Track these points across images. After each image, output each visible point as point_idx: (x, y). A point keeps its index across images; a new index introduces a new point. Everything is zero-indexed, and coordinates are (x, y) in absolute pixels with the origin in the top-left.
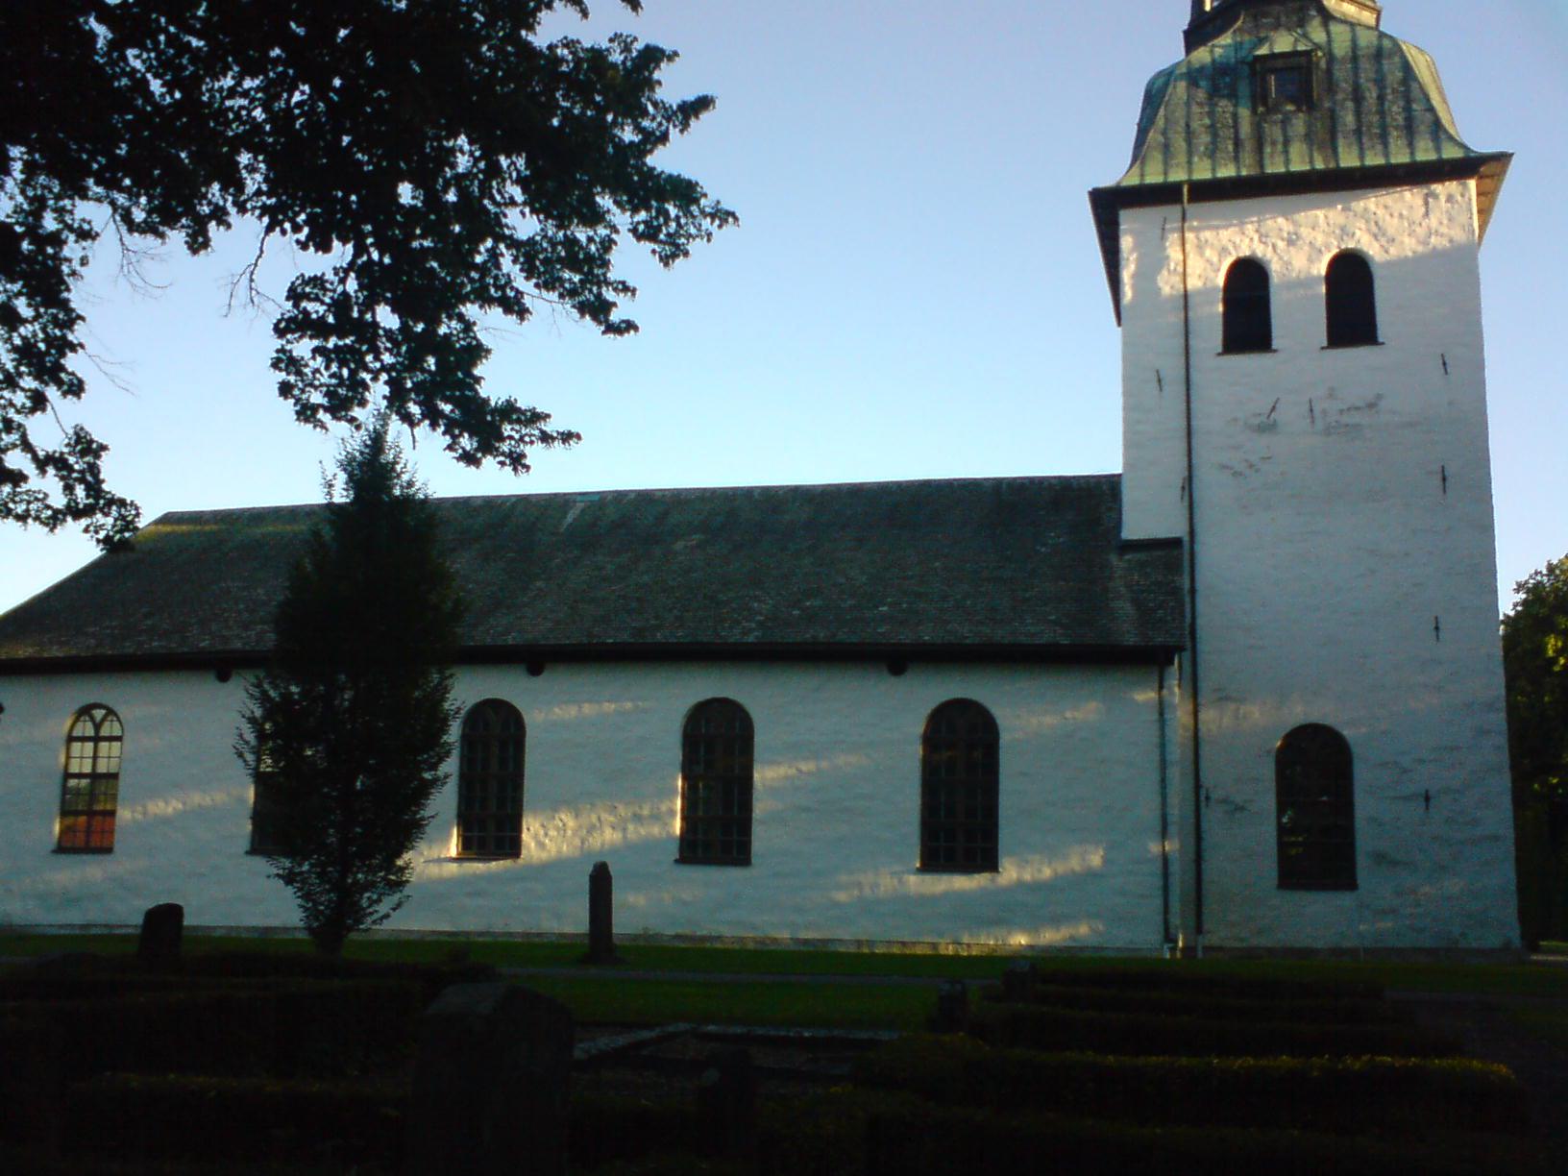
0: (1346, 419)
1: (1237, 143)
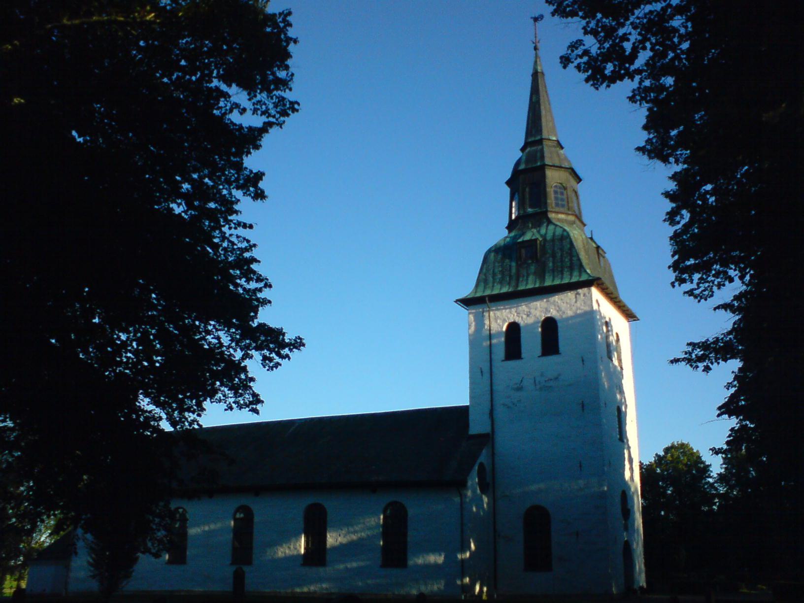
1: (510, 277)
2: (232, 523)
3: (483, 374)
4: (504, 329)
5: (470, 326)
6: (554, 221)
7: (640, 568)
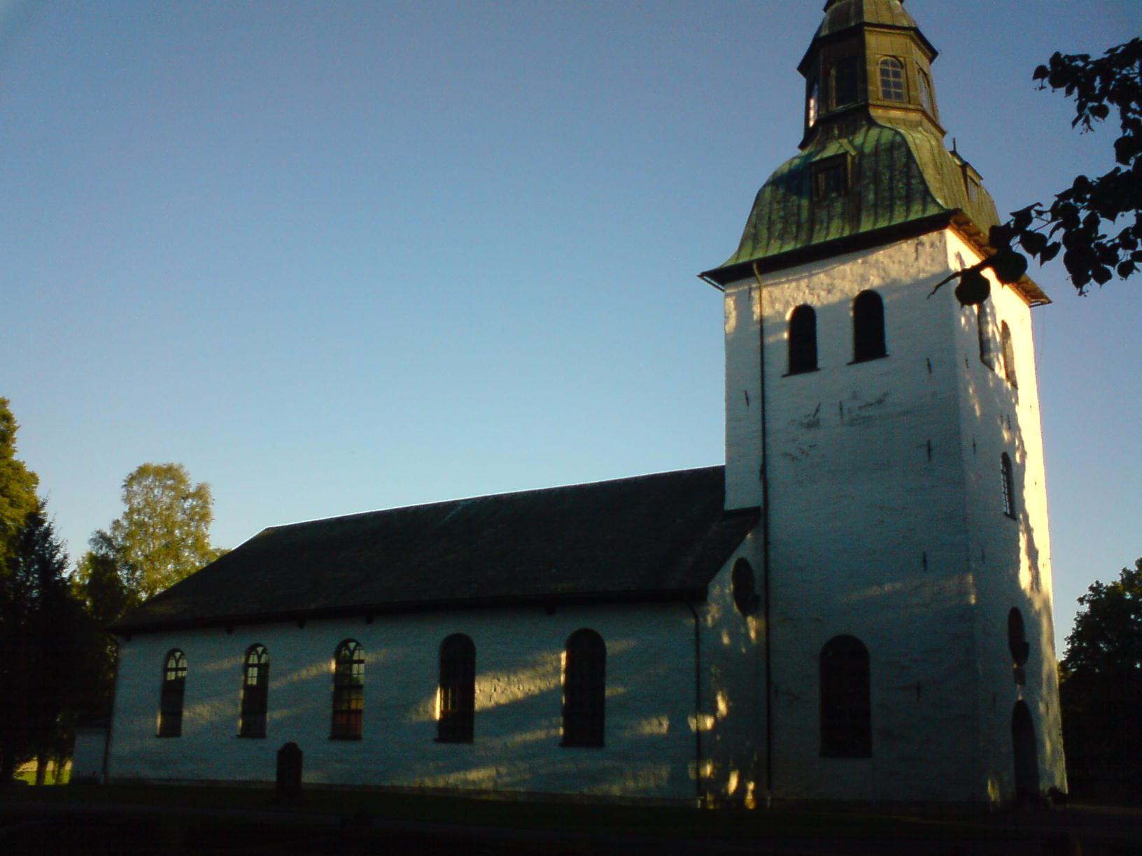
0: (864, 413)
1: (799, 225)
2: (333, 666)
3: (750, 405)
4: (788, 316)
5: (727, 318)
6: (880, 122)
7: (1054, 750)
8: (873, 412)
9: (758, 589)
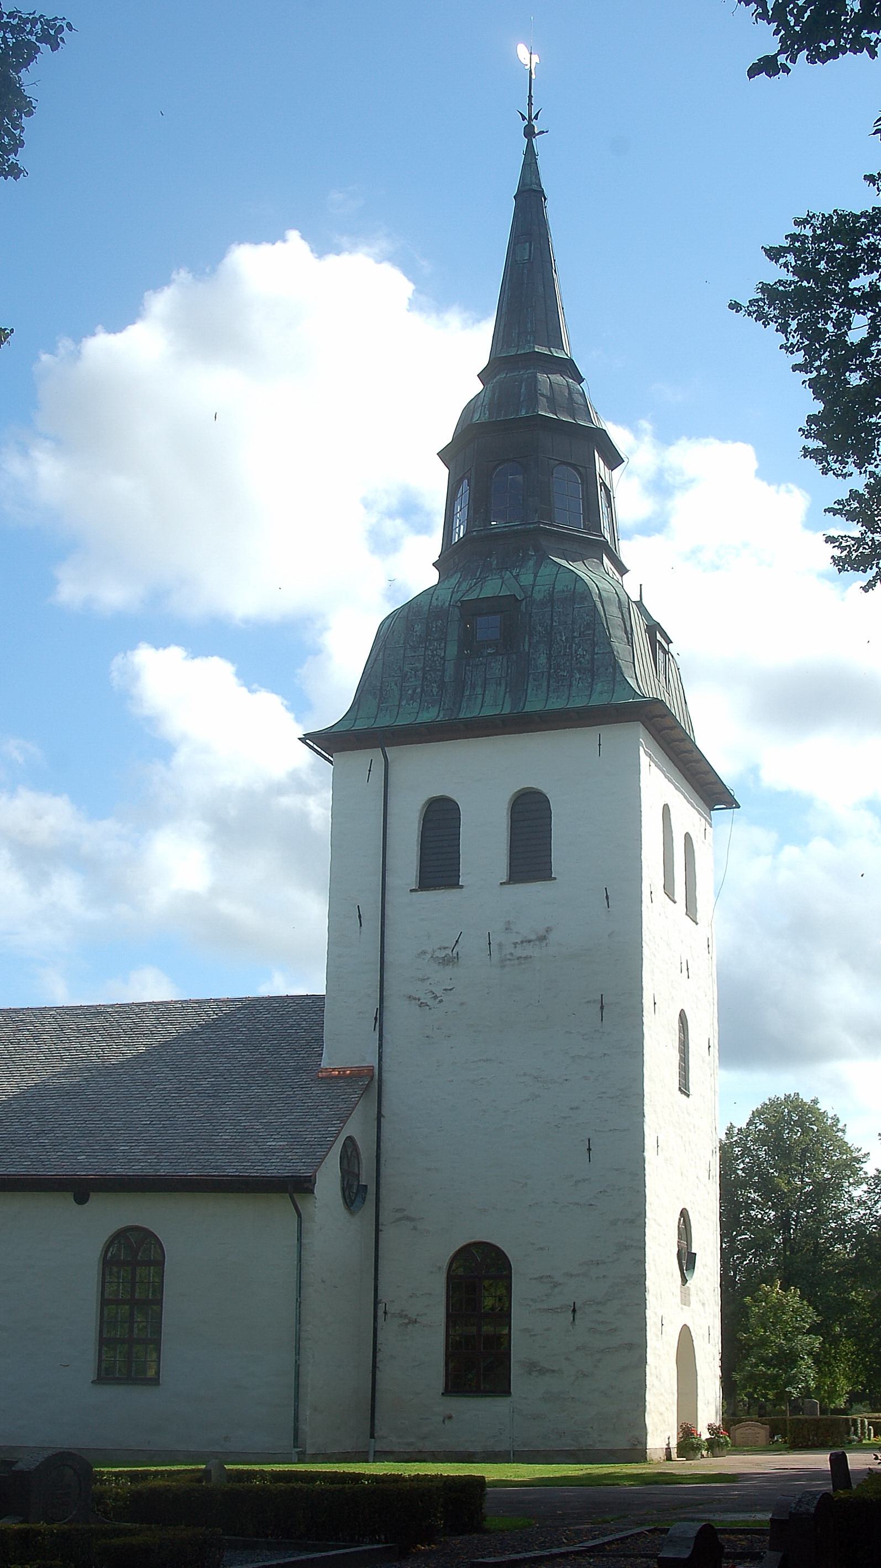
0: (519, 952)
3: (362, 923)
8: (528, 951)
9: (366, 1177)
